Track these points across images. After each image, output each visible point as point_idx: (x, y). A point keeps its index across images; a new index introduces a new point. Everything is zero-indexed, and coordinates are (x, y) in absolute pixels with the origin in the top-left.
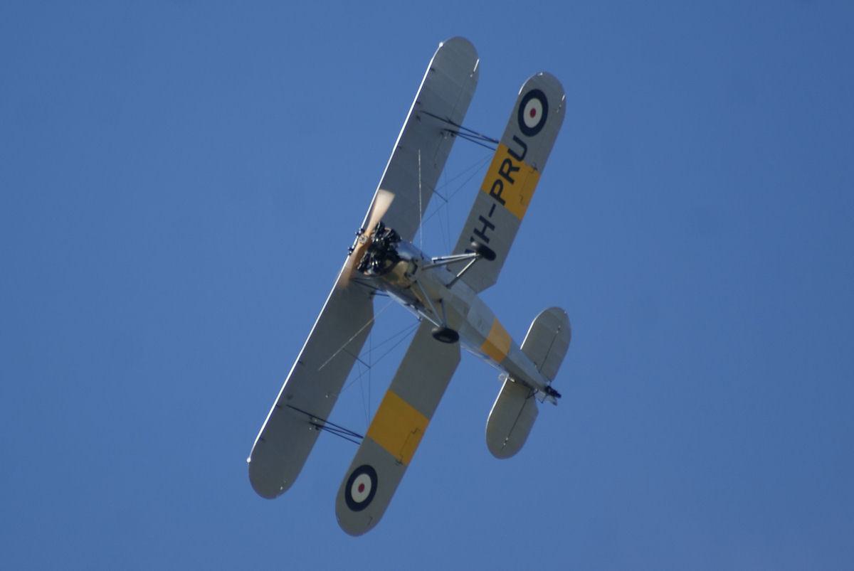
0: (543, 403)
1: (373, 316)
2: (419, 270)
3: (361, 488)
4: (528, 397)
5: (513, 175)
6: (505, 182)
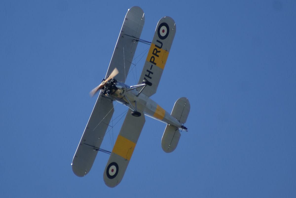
1: (113, 107)
2: (125, 91)
3: (113, 170)
4: (176, 130)
5: (158, 54)
6: (155, 56)
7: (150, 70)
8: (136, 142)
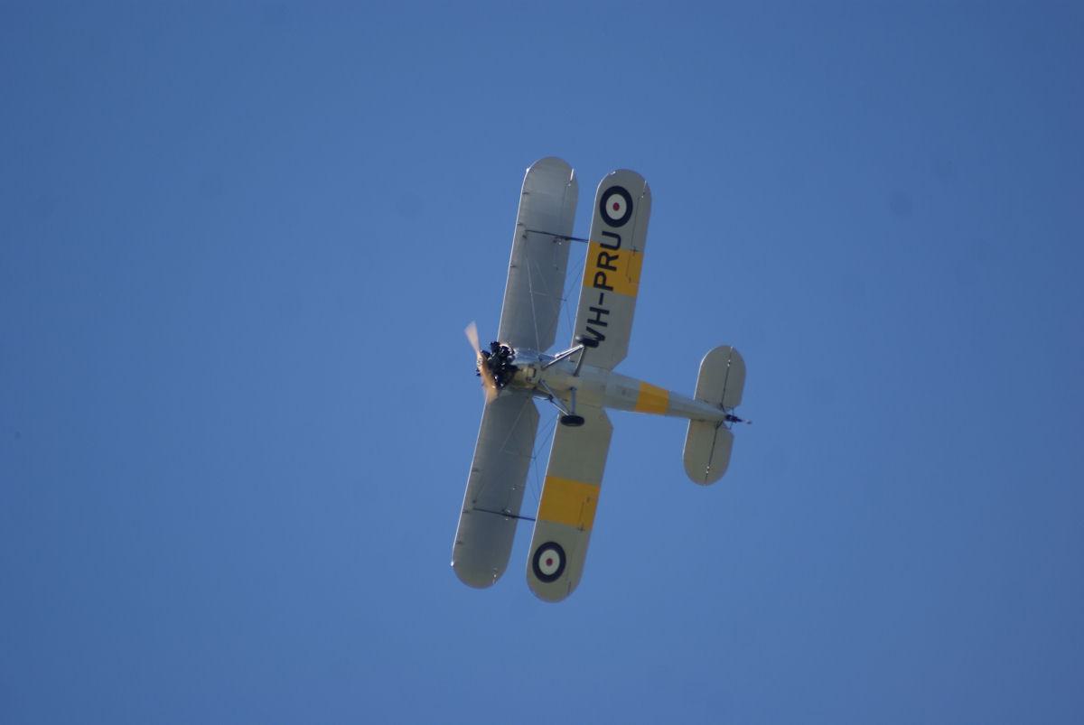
0: (735, 427)
5: (612, 263)
6: (606, 271)
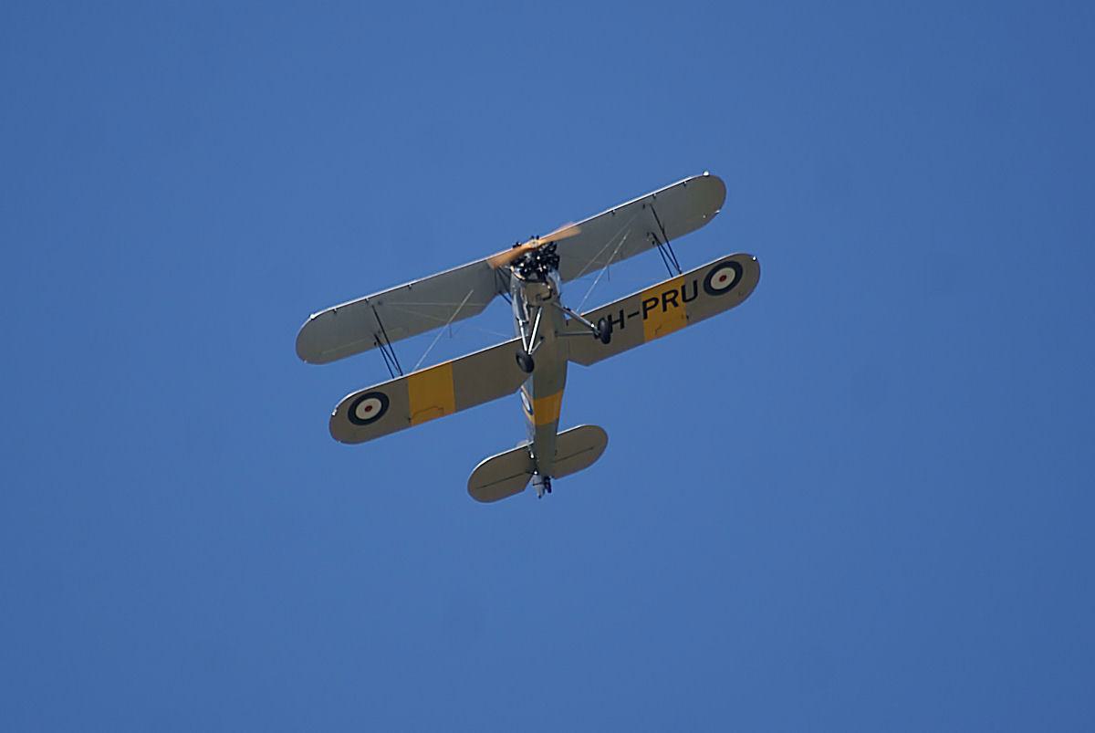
2: (550, 301)
3: (368, 409)
5: (669, 305)
7: (625, 318)
8: (461, 405)
